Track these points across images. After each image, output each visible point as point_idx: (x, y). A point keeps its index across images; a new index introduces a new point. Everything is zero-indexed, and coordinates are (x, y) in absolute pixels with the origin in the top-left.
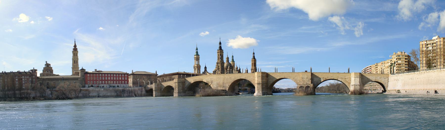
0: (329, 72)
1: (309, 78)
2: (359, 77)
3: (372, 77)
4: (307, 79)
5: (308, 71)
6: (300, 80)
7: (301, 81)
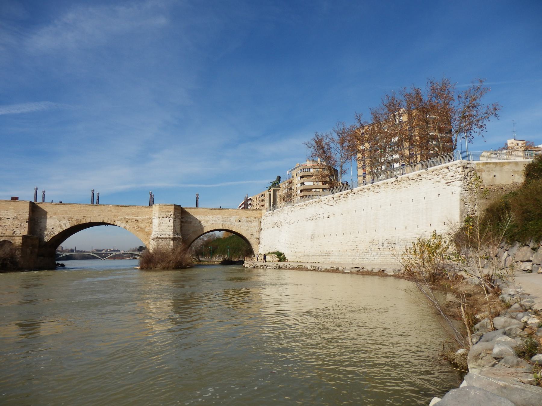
1: (23, 220)
2: (172, 216)
3: (214, 219)
4: (16, 222)
5: (19, 199)
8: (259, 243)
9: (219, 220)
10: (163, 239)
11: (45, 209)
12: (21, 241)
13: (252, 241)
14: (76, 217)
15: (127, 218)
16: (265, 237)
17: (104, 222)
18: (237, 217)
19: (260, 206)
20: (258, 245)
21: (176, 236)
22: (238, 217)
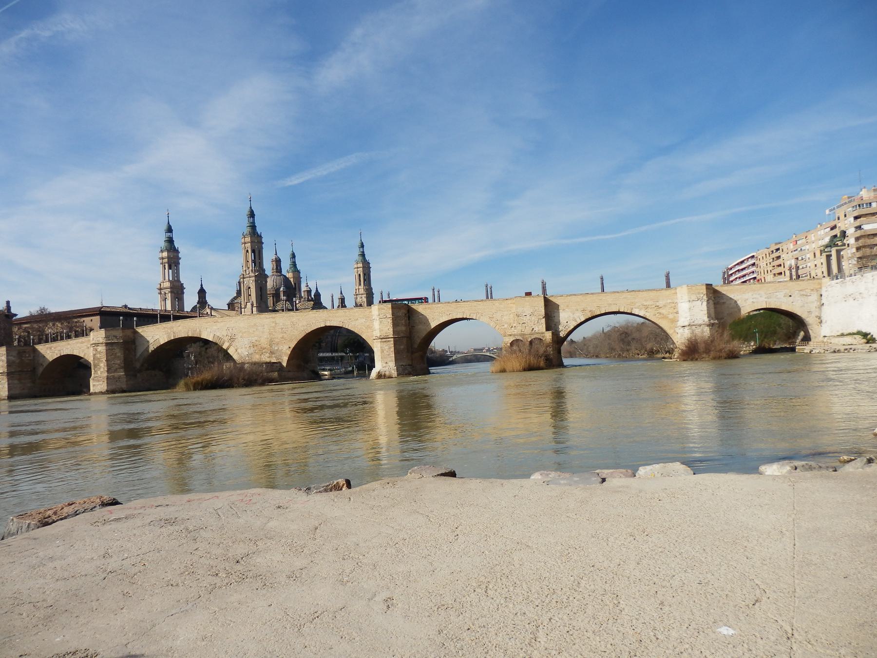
0: (603, 290)
2: (705, 297)
3: (755, 296)
4: (533, 318)
6: (512, 321)
7: (515, 325)
8: (821, 322)
9: (761, 296)
10: (696, 326)
11: (557, 303)
12: (551, 337)
13: (810, 320)
14: (589, 309)
15: (645, 304)
16: (827, 313)
17: (620, 311)
18: (786, 291)
19: (774, 266)
20: (820, 325)
21: (712, 321)
22: (787, 291)
